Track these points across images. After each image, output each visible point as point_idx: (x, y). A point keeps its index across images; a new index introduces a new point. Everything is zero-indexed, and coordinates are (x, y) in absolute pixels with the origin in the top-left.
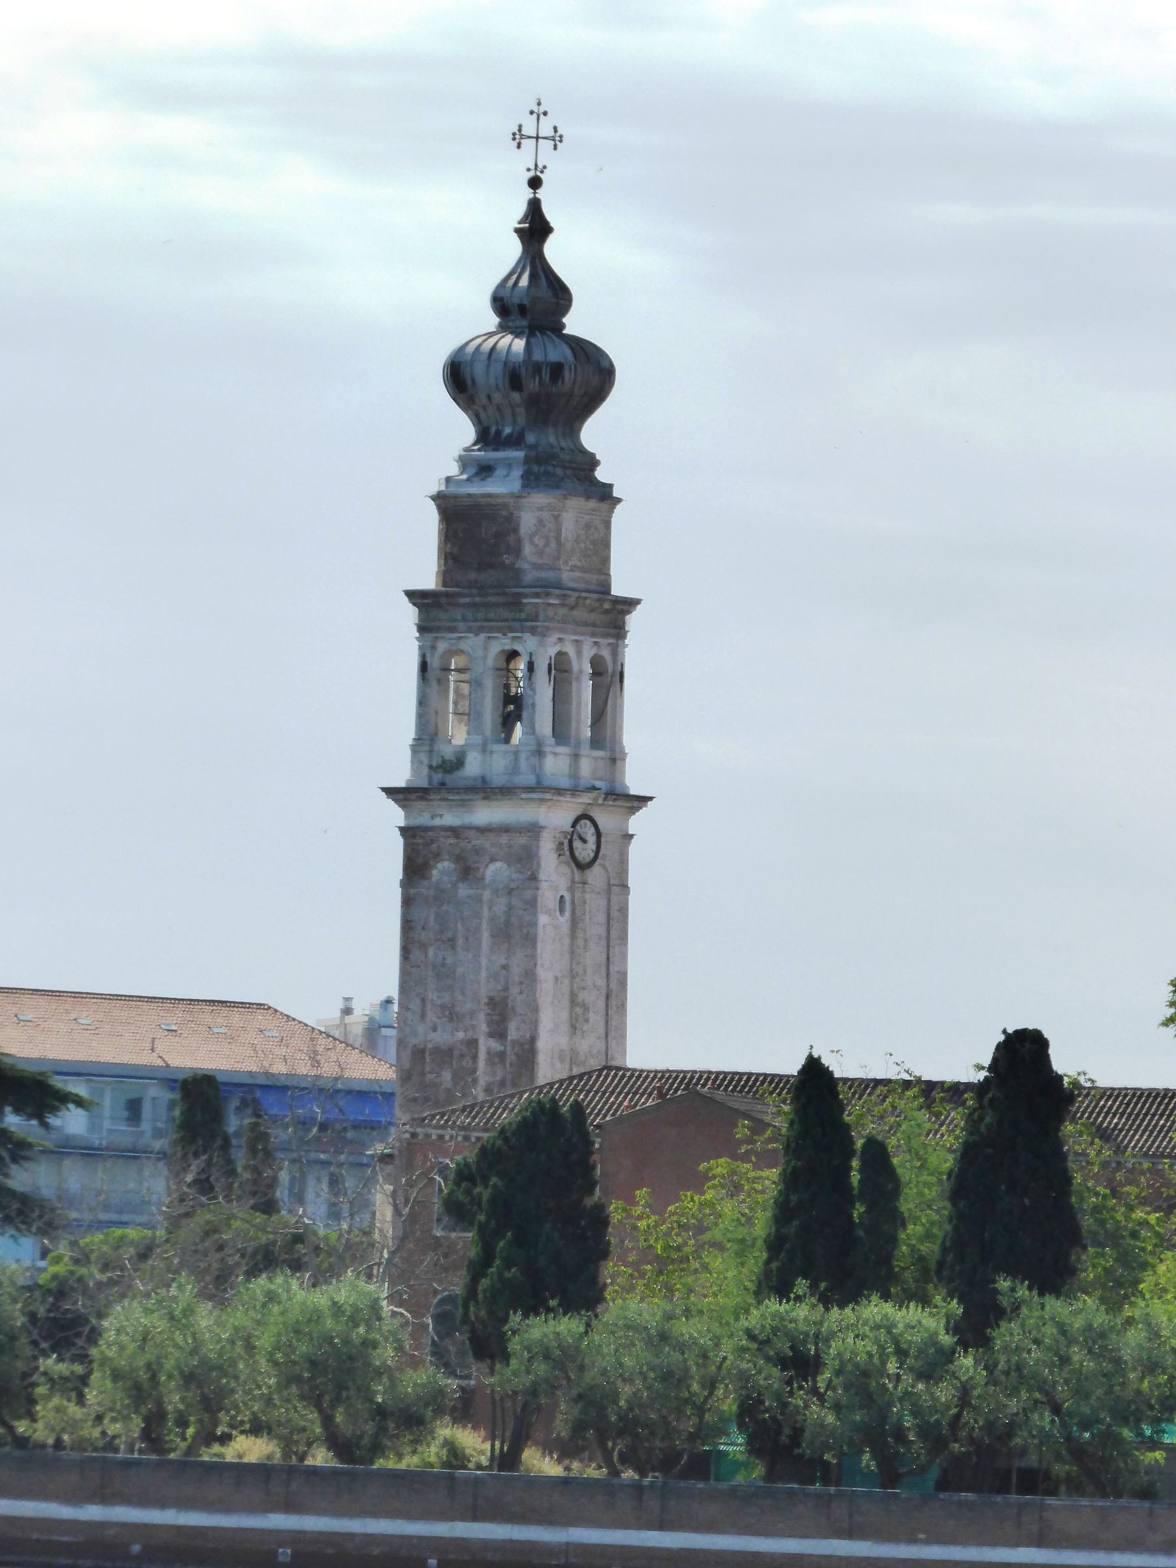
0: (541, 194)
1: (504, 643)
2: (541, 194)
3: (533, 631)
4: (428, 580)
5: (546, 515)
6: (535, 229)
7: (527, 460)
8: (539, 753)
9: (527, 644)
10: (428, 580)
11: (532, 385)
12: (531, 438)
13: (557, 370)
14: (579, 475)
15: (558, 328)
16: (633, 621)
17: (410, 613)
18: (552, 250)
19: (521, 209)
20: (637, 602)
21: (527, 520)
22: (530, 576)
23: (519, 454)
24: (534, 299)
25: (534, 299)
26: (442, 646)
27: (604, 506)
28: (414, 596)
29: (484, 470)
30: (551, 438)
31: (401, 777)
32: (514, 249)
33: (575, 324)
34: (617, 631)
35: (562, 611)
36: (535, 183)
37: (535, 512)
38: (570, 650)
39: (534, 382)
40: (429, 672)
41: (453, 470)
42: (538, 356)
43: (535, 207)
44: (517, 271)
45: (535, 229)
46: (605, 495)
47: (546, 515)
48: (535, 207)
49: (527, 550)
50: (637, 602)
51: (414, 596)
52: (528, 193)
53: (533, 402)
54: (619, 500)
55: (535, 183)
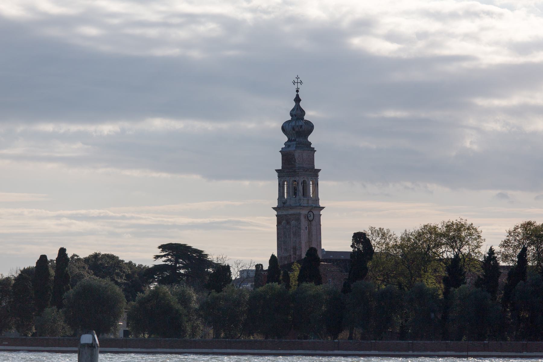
1: (293, 179)
3: (298, 176)
4: (281, 168)
6: (298, 100)
8: (300, 199)
9: (297, 179)
10: (281, 168)
11: (297, 129)
12: (297, 140)
13: (301, 126)
16: (320, 174)
18: (301, 104)
19: (295, 96)
22: (297, 166)
23: (295, 143)
24: (298, 113)
25: (298, 113)
26: (282, 180)
28: (277, 171)
29: (289, 146)
31: (276, 205)
32: (294, 104)
33: (306, 118)
34: (317, 176)
36: (297, 91)
37: (297, 154)
38: (306, 180)
39: (298, 129)
40: (281, 187)
42: (297, 124)
43: (298, 96)
45: (298, 100)
46: (313, 150)
48: (298, 96)
49: (297, 161)
51: (277, 171)
52: (296, 93)
55: (297, 91)
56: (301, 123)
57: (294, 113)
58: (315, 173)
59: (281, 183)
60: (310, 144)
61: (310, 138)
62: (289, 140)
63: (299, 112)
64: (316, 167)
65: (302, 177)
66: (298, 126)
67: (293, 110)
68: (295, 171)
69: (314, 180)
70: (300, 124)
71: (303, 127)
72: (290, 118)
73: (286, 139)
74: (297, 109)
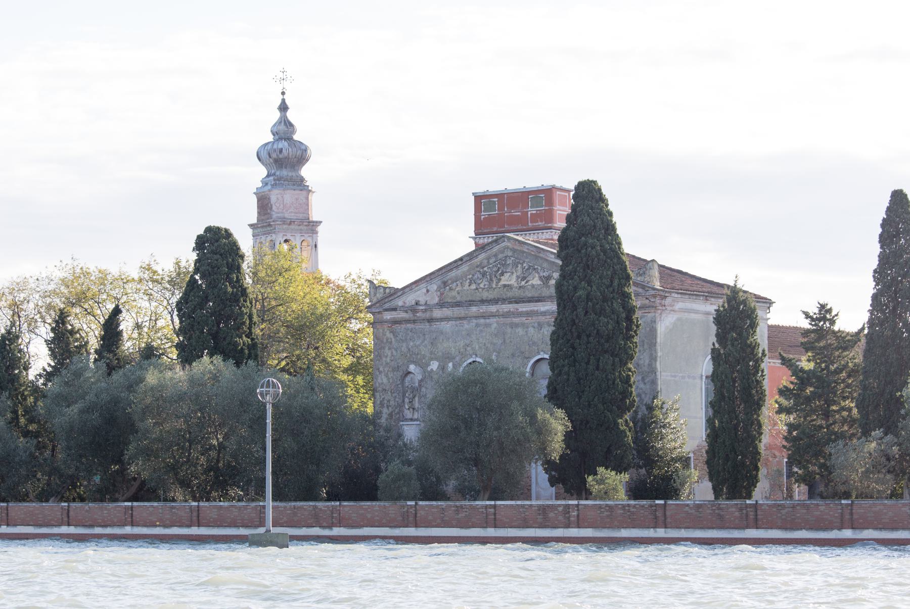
0: (285, 97)
1: (269, 238)
2: (285, 97)
4: (255, 221)
5: (279, 196)
6: (283, 107)
7: (274, 180)
10: (255, 221)
11: (274, 156)
12: (278, 173)
13: (281, 151)
14: (300, 184)
15: (289, 139)
16: (320, 229)
17: (250, 231)
18: (290, 115)
19: (279, 102)
20: (321, 222)
21: (273, 199)
22: (275, 216)
23: (272, 178)
24: (284, 130)
25: (284, 130)
27: (304, 193)
28: (251, 226)
29: (267, 184)
30: (285, 173)
32: (277, 115)
35: (285, 226)
36: (283, 93)
37: (274, 196)
38: (291, 238)
41: (260, 185)
42: (275, 146)
43: (283, 101)
45: (283, 107)
46: (307, 191)
47: (279, 196)
48: (283, 101)
49: (274, 208)
50: (321, 222)
51: (251, 226)
52: (281, 97)
53: (276, 161)
54: (310, 191)
55: (283, 93)
56: (283, 144)
57: (275, 130)
58: (311, 227)
61: (306, 171)
62: (268, 176)
63: (282, 127)
64: (314, 217)
65: (281, 234)
66: (275, 150)
67: (275, 125)
68: (270, 225)
69: (310, 239)
70: (280, 146)
71: (284, 151)
72: (270, 138)
73: (263, 171)
74: (281, 122)
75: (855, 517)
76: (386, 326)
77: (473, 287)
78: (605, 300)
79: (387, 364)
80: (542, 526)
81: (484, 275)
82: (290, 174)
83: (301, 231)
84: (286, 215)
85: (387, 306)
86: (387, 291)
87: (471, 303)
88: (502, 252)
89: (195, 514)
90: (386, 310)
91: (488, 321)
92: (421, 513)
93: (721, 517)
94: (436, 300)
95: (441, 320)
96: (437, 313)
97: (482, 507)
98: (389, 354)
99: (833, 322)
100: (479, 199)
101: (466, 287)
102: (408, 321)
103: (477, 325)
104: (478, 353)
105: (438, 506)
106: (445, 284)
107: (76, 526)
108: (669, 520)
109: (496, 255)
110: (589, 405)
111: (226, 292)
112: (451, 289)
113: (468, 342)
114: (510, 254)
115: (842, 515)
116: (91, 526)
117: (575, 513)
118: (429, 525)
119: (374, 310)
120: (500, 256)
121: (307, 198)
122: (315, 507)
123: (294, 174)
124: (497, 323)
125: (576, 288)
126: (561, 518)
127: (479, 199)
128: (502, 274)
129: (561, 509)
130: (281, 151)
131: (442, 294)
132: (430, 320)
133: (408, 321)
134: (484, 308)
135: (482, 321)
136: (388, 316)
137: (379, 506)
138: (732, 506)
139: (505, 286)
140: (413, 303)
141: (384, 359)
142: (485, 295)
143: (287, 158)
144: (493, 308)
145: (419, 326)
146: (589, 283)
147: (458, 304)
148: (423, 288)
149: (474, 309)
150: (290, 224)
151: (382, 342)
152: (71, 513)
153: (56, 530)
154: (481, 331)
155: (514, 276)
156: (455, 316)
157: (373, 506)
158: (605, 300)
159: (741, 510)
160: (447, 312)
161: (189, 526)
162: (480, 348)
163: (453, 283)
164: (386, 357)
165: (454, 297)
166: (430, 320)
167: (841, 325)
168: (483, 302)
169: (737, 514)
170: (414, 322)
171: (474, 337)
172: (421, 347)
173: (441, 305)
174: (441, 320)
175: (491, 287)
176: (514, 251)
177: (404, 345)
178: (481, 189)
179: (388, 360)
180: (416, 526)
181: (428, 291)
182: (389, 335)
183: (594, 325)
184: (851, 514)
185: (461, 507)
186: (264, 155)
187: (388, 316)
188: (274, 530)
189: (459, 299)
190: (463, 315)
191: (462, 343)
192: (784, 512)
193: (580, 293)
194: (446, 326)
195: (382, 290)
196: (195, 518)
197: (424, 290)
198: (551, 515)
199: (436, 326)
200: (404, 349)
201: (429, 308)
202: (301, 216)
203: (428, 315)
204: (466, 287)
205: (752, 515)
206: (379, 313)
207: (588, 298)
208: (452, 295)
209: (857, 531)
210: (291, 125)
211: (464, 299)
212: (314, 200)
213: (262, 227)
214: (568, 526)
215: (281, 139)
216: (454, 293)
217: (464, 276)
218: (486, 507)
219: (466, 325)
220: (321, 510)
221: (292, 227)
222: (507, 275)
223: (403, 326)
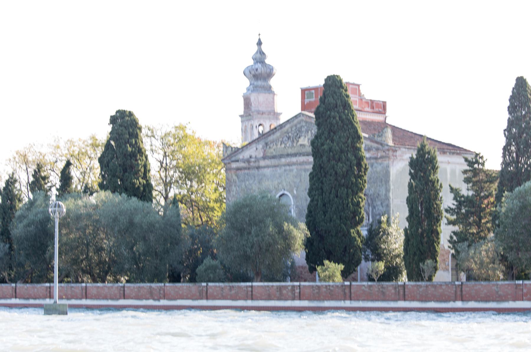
1: (250, 123)
4: (242, 113)
6: (260, 43)
10: (242, 113)
11: (253, 73)
14: (269, 89)
17: (240, 119)
18: (263, 47)
19: (257, 41)
21: (252, 99)
22: (253, 109)
24: (260, 57)
25: (260, 57)
27: (271, 95)
30: (260, 83)
43: (260, 40)
44: (257, 52)
45: (260, 43)
48: (260, 40)
49: (253, 104)
56: (259, 66)
59: (243, 128)
60: (270, 87)
61: (273, 82)
63: (258, 55)
64: (279, 111)
68: (250, 115)
70: (256, 66)
72: (251, 62)
75: (464, 293)
76: (233, 172)
77: (283, 146)
78: (342, 151)
79: (233, 196)
80: (279, 299)
81: (289, 138)
82: (263, 84)
83: (269, 119)
84: (260, 109)
85: (233, 159)
86: (233, 149)
87: (281, 156)
88: (299, 123)
89: (84, 291)
90: (233, 161)
91: (291, 168)
92: (210, 291)
93: (383, 293)
94: (261, 155)
95: (264, 167)
96: (262, 163)
97: (245, 287)
98: (235, 189)
99: (483, 164)
100: (303, 91)
101: (279, 146)
102: (245, 168)
103: (285, 170)
104: (286, 188)
105: (219, 287)
106: (267, 144)
107: (20, 298)
108: (353, 295)
109: (296, 126)
110: (331, 220)
111: (127, 150)
112: (270, 147)
113: (279, 181)
114: (304, 124)
115: (456, 291)
116: (28, 299)
117: (298, 291)
118: (214, 298)
119: (226, 161)
120: (298, 126)
121: (274, 99)
122: (151, 287)
123: (265, 84)
124: (297, 169)
125: (323, 145)
126: (290, 294)
127: (303, 91)
128: (299, 137)
129: (290, 288)
130: (257, 70)
131: (265, 151)
132: (258, 168)
133: (245, 168)
134: (289, 160)
135: (288, 168)
136: (234, 165)
137: (187, 286)
138: (390, 286)
139: (301, 145)
140: (249, 157)
141: (232, 193)
142: (290, 151)
143: (261, 74)
144: (294, 159)
145: (252, 172)
146: (332, 141)
147: (274, 157)
148: (254, 146)
149: (283, 160)
150: (263, 114)
151: (231, 182)
152: (18, 291)
153: (9, 301)
154: (287, 174)
155: (307, 139)
156: (273, 164)
157: (183, 286)
158: (342, 151)
159: (395, 288)
160: (268, 162)
161: (81, 299)
162: (287, 185)
163: (271, 143)
164: (233, 191)
165: (272, 153)
166: (258, 168)
167: (488, 166)
168: (288, 155)
169: (393, 291)
170: (249, 169)
171: (283, 178)
172: (253, 185)
173: (264, 158)
174: (264, 167)
175: (293, 146)
176: (306, 122)
177: (243, 184)
178: (305, 86)
179: (234, 193)
180: (207, 299)
181: (257, 149)
182: (235, 177)
183: (333, 167)
184: (462, 291)
185: (233, 287)
186: (247, 72)
187: (234, 165)
188: (59, 302)
189: (274, 153)
190: (277, 164)
191: (276, 183)
192: (421, 290)
193: (326, 147)
194: (267, 171)
195: (230, 149)
196: (84, 294)
197: (255, 149)
198: (284, 292)
199: (262, 171)
200: (243, 186)
201: (257, 160)
202: (269, 109)
203: (257, 164)
204: (279, 146)
205: (401, 293)
206: (229, 163)
207: (330, 150)
208: (271, 151)
209: (465, 303)
210: (264, 54)
211: (278, 153)
212: (278, 100)
213: (246, 116)
214: (293, 299)
215: (257, 62)
216: (272, 150)
217: (278, 139)
218: (247, 287)
219: (279, 170)
220: (154, 288)
221: (264, 116)
222: (302, 138)
223: (243, 172)
